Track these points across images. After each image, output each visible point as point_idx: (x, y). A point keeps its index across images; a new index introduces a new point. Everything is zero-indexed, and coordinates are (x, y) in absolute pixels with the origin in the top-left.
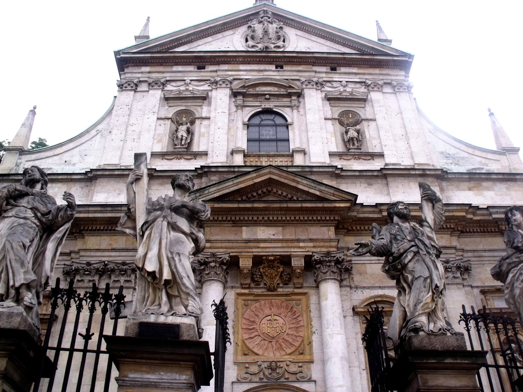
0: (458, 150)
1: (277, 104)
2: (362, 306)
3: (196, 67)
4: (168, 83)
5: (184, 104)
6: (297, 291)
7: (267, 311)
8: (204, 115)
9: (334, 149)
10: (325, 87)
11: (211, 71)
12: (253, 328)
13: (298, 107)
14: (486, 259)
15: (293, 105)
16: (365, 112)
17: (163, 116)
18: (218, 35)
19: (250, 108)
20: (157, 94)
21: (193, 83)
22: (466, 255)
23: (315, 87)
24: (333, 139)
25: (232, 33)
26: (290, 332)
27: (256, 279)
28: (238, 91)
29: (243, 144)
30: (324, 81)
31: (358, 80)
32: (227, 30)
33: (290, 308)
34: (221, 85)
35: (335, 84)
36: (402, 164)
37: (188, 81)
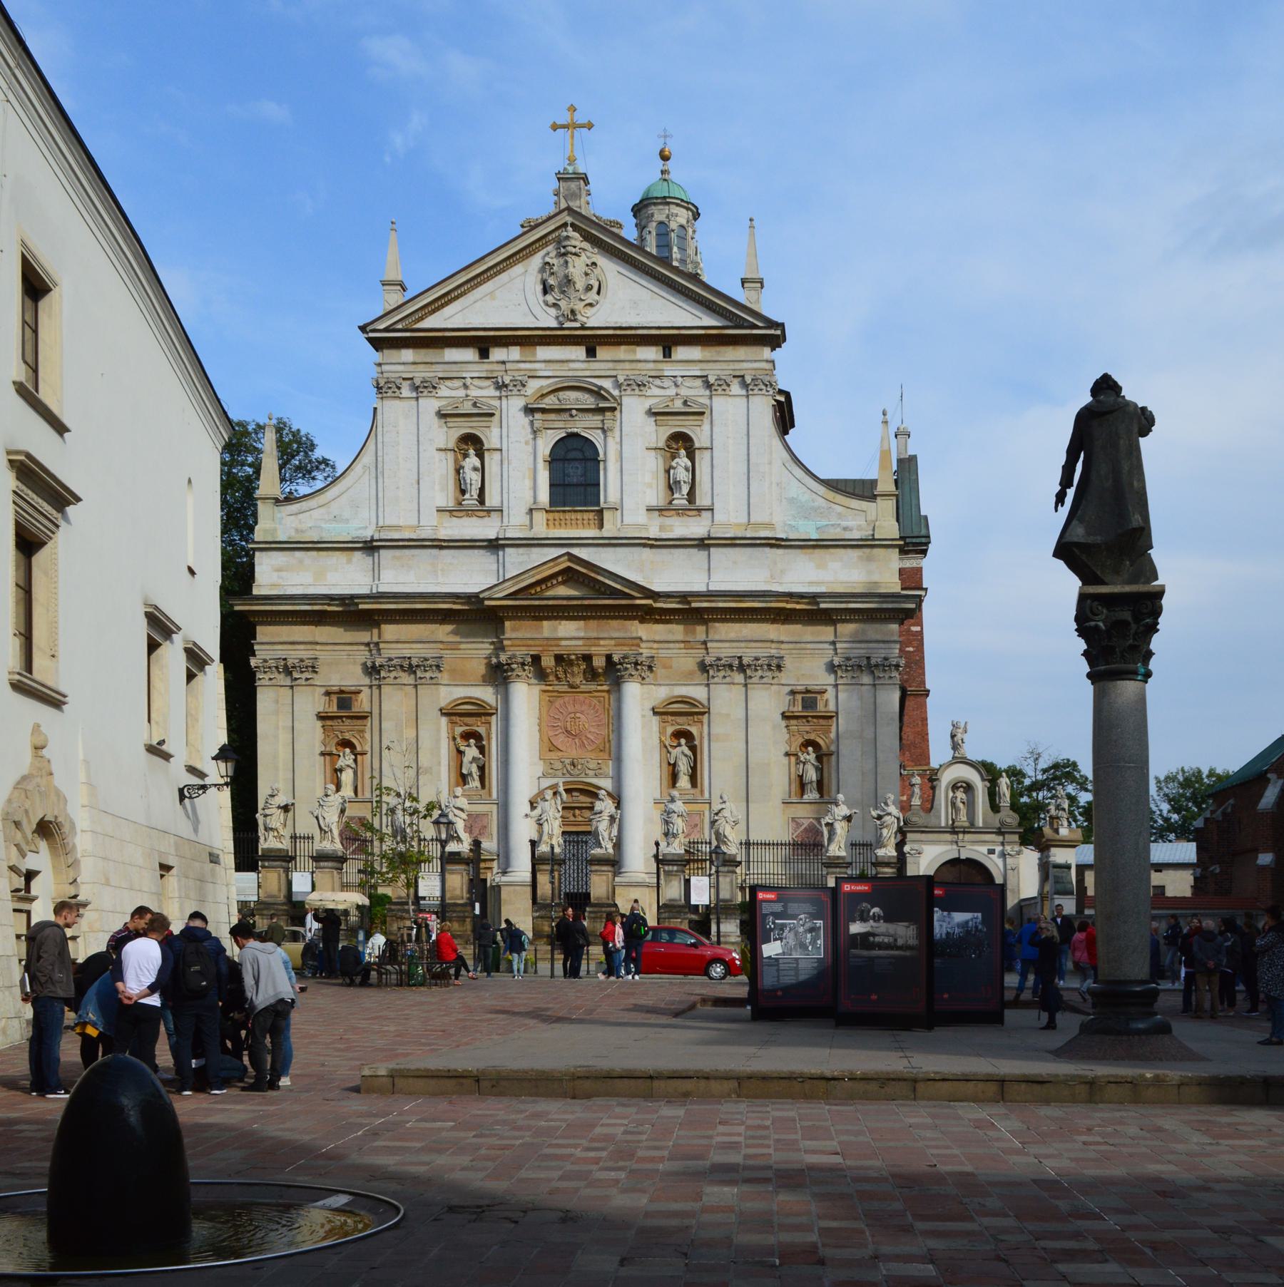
3: (477, 351)
4: (442, 381)
6: (599, 688)
7: (571, 709)
9: (654, 503)
11: (498, 362)
14: (808, 652)
15: (606, 428)
16: (700, 437)
17: (443, 447)
19: (552, 431)
20: (430, 405)
21: (476, 382)
22: (783, 646)
23: (637, 392)
24: (655, 481)
25: (523, 271)
26: (593, 730)
28: (535, 406)
29: (544, 496)
30: (652, 377)
31: (698, 373)
32: (515, 264)
34: (511, 390)
35: (667, 383)
36: (733, 520)
37: (468, 381)
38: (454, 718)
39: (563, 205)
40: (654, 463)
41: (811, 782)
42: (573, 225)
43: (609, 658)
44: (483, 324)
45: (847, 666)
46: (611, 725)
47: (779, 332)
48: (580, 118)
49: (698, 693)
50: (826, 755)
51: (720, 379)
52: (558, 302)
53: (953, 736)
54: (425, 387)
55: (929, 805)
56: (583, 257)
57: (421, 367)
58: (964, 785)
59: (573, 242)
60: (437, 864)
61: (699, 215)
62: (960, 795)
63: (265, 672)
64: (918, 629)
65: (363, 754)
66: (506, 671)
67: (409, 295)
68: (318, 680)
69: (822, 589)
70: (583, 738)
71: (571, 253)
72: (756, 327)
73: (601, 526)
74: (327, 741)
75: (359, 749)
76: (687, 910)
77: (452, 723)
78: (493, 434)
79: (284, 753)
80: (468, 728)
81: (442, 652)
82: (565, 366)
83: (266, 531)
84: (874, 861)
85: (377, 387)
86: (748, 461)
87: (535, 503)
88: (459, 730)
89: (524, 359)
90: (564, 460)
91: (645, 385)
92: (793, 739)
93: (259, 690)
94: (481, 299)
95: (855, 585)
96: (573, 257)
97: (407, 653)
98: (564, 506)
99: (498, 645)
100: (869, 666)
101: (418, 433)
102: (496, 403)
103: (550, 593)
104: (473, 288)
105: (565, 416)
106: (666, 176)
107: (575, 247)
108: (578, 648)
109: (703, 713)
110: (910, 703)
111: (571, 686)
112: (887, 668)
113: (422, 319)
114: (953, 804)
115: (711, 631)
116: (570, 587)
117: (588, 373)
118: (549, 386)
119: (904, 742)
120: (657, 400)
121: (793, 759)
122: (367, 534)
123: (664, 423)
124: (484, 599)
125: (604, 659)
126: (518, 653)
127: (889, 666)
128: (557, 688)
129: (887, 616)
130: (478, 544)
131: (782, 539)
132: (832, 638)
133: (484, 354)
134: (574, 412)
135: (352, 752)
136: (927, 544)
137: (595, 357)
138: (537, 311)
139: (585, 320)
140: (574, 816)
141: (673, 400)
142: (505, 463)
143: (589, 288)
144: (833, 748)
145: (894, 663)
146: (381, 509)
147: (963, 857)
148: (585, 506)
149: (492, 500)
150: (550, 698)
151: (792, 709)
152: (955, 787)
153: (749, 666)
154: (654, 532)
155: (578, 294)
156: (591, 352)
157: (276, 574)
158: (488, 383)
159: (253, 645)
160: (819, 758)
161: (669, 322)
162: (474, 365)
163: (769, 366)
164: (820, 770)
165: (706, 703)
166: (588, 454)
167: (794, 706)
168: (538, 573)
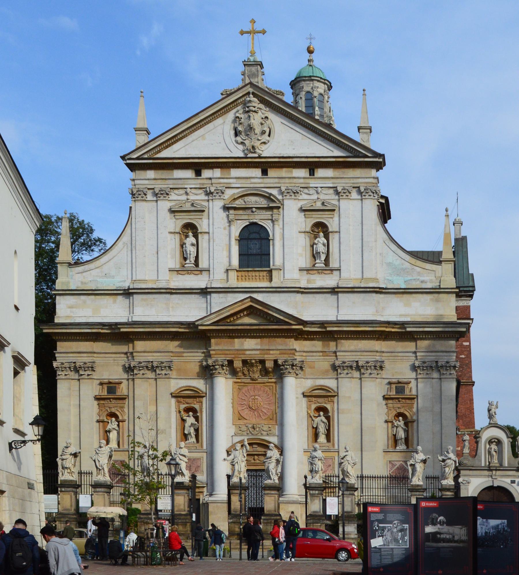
0: (403, 261)
1: (262, 217)
2: (308, 392)
4: (172, 190)
5: (187, 217)
6: (270, 380)
7: (252, 393)
8: (204, 231)
9: (303, 265)
10: (302, 194)
11: (207, 179)
12: (244, 404)
13: (277, 221)
14: (399, 358)
15: (274, 219)
16: (332, 225)
17: (173, 231)
18: (210, 124)
19: (240, 221)
20: (164, 205)
21: (193, 191)
22: (384, 354)
23: (293, 197)
24: (304, 252)
26: (266, 407)
27: (245, 373)
29: (235, 262)
30: (302, 188)
31: (331, 185)
32: (218, 118)
33: (266, 391)
34: (215, 196)
35: (312, 191)
36: (352, 277)
37: (189, 190)
38: (179, 399)
39: (247, 81)
40: (303, 241)
41: (401, 439)
42: (253, 94)
43: (276, 361)
44: (198, 155)
45: (423, 367)
46: (277, 403)
47: (381, 160)
48: (258, 27)
49: (331, 383)
50: (410, 422)
51: (345, 189)
52: (244, 141)
53: (489, 410)
54: (162, 194)
55: (474, 453)
56: (260, 113)
57: (159, 182)
58: (496, 440)
59: (254, 104)
60: (169, 489)
61: (332, 87)
62: (494, 447)
63: (62, 371)
64: (468, 344)
65: (123, 421)
66: (212, 370)
67: (152, 137)
68: (95, 375)
69: (408, 319)
70: (260, 411)
71: (252, 111)
72: (366, 157)
73: (271, 280)
74: (101, 413)
75: (120, 418)
76: (324, 518)
77: (179, 402)
78: (203, 223)
79: (74, 421)
80: (320, 405)
81: (172, 358)
82: (248, 181)
83: (63, 283)
84: (440, 487)
85: (132, 194)
86: (362, 239)
87: (230, 266)
88: (183, 406)
89: (223, 177)
90: (248, 239)
91: (298, 193)
92: (390, 412)
93: (58, 381)
94: (196, 139)
95: (428, 316)
96: (254, 113)
97: (150, 359)
98: (248, 268)
99: (207, 354)
100: (437, 367)
101: (157, 223)
102: (205, 204)
103: (239, 322)
104: (191, 133)
105: (249, 212)
106: (311, 63)
107: (254, 107)
108: (257, 356)
109: (334, 396)
110: (462, 390)
111: (252, 379)
112: (448, 368)
113: (159, 152)
114: (490, 453)
115: (339, 345)
116: (251, 318)
117: (262, 185)
118: (238, 193)
119: (459, 414)
120: (305, 202)
121: (390, 424)
122: (126, 285)
123: (310, 216)
124: (198, 325)
125: (273, 362)
126: (219, 359)
127: (450, 367)
128: (243, 380)
129: (448, 336)
130: (194, 291)
131: (383, 288)
132: (414, 350)
133: (198, 173)
134: (254, 209)
135: (116, 420)
136: (473, 291)
137: (267, 175)
138: (232, 146)
139: (261, 152)
140: (254, 460)
141: (315, 202)
142: (211, 241)
143: (263, 133)
144: (415, 418)
145: (453, 365)
146: (134, 270)
147: (495, 485)
148: (261, 268)
149: (203, 264)
150: (239, 387)
151: (389, 393)
152: (490, 442)
153: (363, 367)
154: (303, 284)
155: (256, 136)
156: (265, 172)
157: (69, 309)
158: (200, 191)
159: (55, 354)
160: (406, 424)
161: (313, 153)
162: (193, 180)
163: (375, 181)
164: (406, 432)
165: (336, 390)
166: (263, 235)
167: (391, 392)
168: (231, 309)
